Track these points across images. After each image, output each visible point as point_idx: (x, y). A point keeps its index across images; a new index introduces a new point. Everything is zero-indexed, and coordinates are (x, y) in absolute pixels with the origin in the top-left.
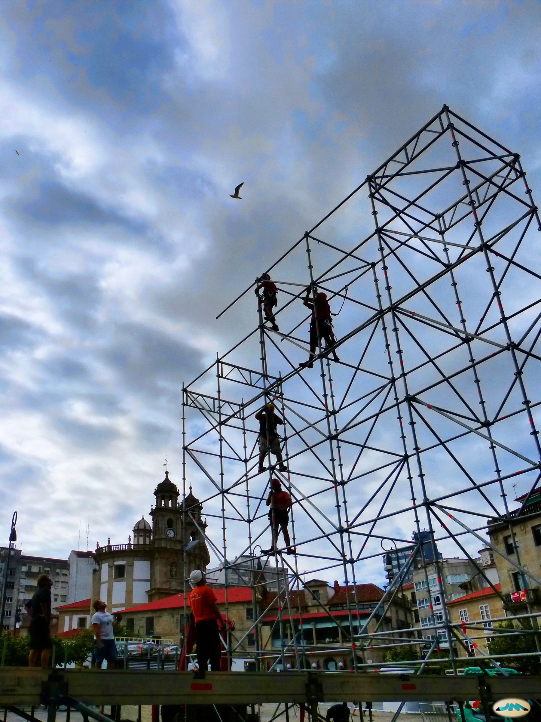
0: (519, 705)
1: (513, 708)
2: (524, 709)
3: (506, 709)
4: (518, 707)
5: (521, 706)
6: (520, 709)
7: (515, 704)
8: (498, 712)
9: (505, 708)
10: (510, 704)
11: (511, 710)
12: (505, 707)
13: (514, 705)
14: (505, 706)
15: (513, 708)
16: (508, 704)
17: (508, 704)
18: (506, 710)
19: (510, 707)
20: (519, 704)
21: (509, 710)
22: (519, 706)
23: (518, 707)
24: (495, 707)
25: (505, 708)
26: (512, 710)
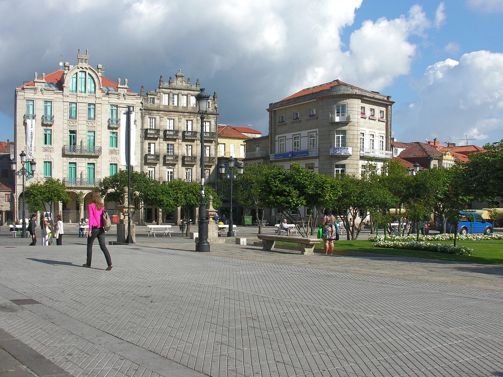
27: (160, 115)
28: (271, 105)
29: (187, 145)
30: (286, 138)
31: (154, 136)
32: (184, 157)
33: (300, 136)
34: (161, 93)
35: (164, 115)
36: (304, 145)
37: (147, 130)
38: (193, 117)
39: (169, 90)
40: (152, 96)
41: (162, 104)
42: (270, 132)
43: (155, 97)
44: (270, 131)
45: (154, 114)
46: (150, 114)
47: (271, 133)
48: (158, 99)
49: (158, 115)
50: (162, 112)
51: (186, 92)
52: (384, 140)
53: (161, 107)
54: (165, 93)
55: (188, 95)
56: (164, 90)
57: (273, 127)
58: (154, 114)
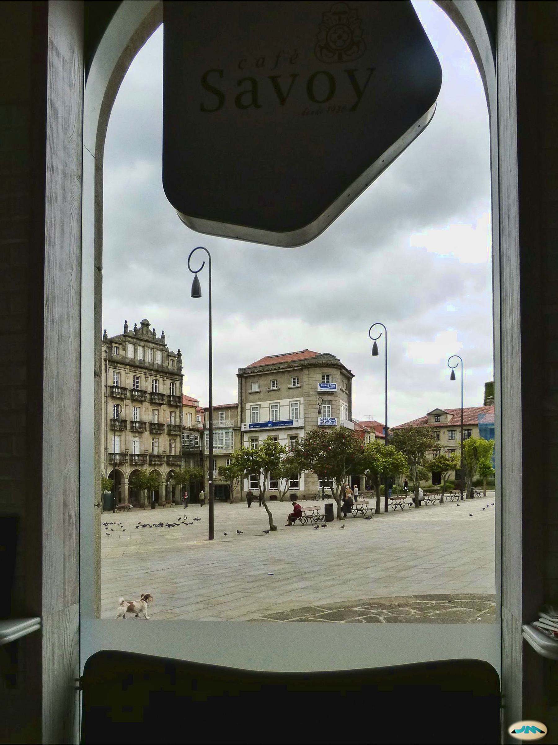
0: (536, 727)
1: (530, 731)
2: (540, 731)
3: (522, 732)
4: (534, 729)
5: (537, 728)
6: (537, 731)
7: (531, 727)
8: (513, 735)
9: (521, 731)
10: (526, 726)
11: (527, 732)
12: (521, 730)
13: (530, 727)
14: (521, 728)
15: (530, 731)
16: (524, 726)
17: (524, 727)
18: (522, 733)
19: (526, 730)
20: (536, 726)
21: (525, 733)
22: (535, 728)
23: (534, 729)
24: (511, 729)
25: (521, 731)
26: (528, 733)
27: (125, 369)
28: (240, 370)
29: (153, 410)
30: (260, 407)
31: (121, 396)
32: (151, 424)
33: (280, 404)
34: (127, 343)
35: (131, 371)
36: (284, 415)
37: (112, 387)
38: (159, 376)
39: (135, 340)
40: (117, 345)
41: (128, 356)
42: (240, 399)
43: (120, 346)
44: (240, 398)
45: (120, 368)
46: (115, 368)
47: (241, 401)
48: (124, 349)
49: (123, 369)
50: (128, 367)
51: (152, 345)
52: (347, 412)
53: (128, 361)
54: (130, 342)
55: (155, 349)
56: (130, 339)
57: (244, 394)
58: (120, 368)
